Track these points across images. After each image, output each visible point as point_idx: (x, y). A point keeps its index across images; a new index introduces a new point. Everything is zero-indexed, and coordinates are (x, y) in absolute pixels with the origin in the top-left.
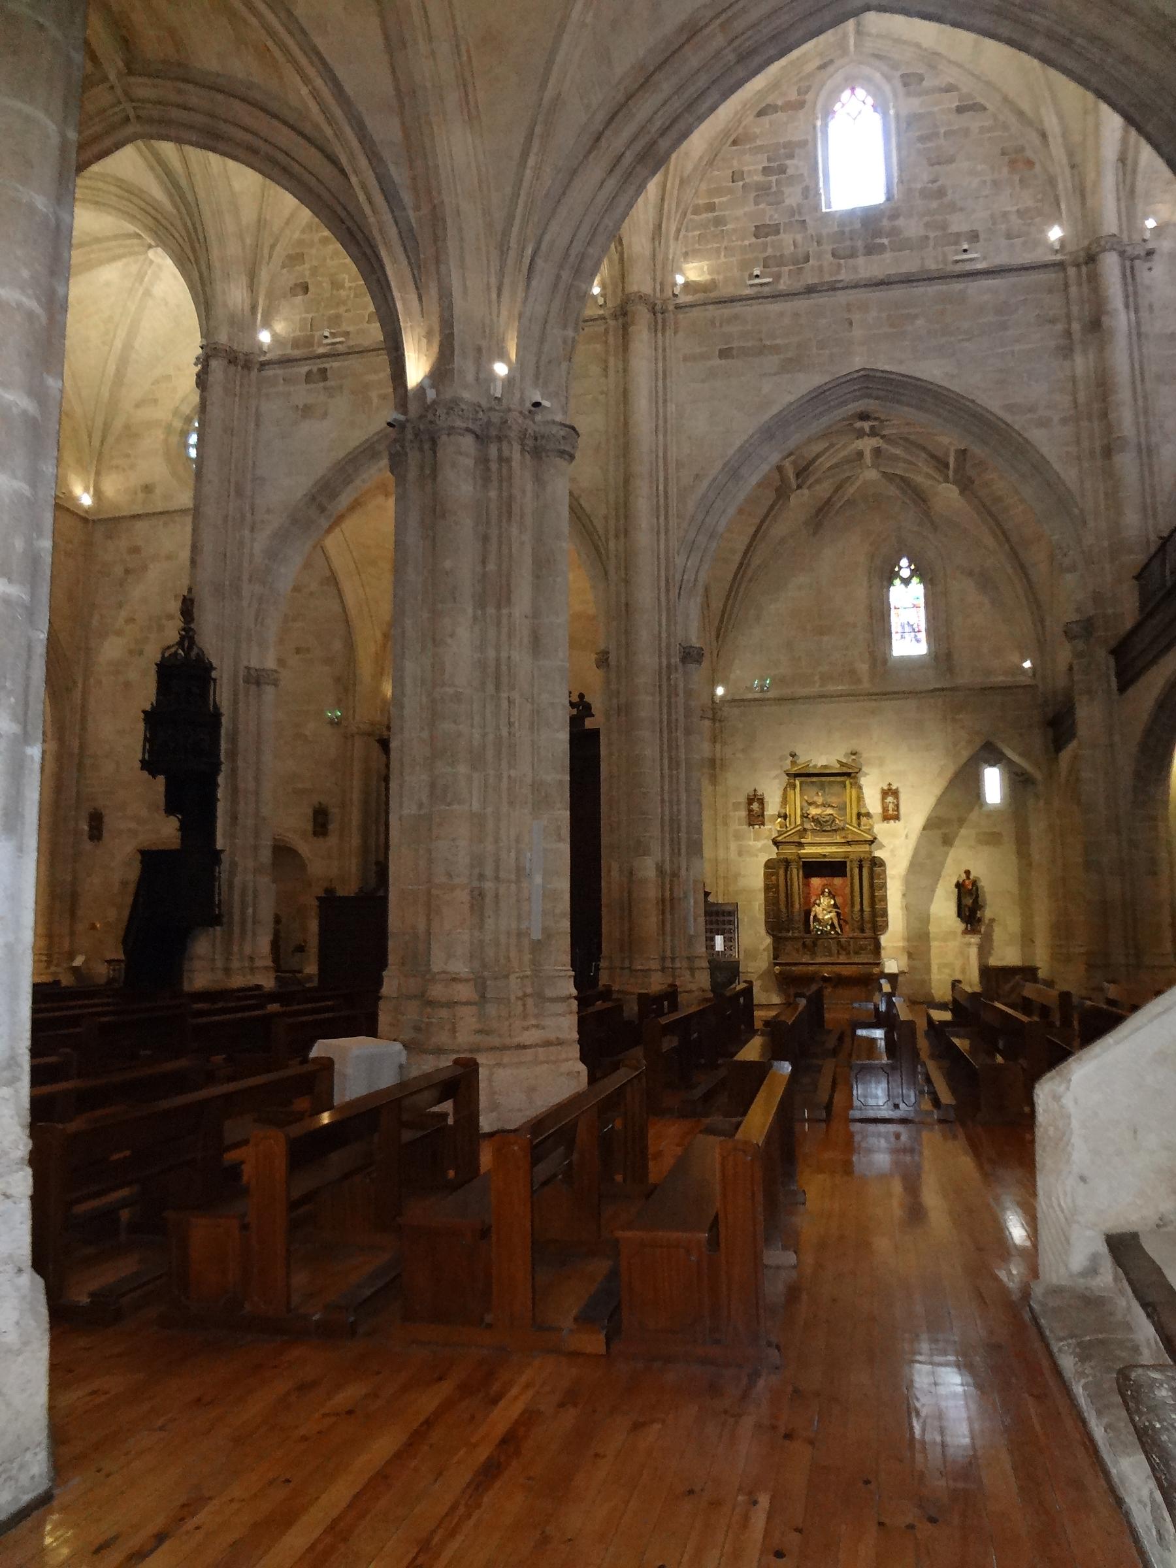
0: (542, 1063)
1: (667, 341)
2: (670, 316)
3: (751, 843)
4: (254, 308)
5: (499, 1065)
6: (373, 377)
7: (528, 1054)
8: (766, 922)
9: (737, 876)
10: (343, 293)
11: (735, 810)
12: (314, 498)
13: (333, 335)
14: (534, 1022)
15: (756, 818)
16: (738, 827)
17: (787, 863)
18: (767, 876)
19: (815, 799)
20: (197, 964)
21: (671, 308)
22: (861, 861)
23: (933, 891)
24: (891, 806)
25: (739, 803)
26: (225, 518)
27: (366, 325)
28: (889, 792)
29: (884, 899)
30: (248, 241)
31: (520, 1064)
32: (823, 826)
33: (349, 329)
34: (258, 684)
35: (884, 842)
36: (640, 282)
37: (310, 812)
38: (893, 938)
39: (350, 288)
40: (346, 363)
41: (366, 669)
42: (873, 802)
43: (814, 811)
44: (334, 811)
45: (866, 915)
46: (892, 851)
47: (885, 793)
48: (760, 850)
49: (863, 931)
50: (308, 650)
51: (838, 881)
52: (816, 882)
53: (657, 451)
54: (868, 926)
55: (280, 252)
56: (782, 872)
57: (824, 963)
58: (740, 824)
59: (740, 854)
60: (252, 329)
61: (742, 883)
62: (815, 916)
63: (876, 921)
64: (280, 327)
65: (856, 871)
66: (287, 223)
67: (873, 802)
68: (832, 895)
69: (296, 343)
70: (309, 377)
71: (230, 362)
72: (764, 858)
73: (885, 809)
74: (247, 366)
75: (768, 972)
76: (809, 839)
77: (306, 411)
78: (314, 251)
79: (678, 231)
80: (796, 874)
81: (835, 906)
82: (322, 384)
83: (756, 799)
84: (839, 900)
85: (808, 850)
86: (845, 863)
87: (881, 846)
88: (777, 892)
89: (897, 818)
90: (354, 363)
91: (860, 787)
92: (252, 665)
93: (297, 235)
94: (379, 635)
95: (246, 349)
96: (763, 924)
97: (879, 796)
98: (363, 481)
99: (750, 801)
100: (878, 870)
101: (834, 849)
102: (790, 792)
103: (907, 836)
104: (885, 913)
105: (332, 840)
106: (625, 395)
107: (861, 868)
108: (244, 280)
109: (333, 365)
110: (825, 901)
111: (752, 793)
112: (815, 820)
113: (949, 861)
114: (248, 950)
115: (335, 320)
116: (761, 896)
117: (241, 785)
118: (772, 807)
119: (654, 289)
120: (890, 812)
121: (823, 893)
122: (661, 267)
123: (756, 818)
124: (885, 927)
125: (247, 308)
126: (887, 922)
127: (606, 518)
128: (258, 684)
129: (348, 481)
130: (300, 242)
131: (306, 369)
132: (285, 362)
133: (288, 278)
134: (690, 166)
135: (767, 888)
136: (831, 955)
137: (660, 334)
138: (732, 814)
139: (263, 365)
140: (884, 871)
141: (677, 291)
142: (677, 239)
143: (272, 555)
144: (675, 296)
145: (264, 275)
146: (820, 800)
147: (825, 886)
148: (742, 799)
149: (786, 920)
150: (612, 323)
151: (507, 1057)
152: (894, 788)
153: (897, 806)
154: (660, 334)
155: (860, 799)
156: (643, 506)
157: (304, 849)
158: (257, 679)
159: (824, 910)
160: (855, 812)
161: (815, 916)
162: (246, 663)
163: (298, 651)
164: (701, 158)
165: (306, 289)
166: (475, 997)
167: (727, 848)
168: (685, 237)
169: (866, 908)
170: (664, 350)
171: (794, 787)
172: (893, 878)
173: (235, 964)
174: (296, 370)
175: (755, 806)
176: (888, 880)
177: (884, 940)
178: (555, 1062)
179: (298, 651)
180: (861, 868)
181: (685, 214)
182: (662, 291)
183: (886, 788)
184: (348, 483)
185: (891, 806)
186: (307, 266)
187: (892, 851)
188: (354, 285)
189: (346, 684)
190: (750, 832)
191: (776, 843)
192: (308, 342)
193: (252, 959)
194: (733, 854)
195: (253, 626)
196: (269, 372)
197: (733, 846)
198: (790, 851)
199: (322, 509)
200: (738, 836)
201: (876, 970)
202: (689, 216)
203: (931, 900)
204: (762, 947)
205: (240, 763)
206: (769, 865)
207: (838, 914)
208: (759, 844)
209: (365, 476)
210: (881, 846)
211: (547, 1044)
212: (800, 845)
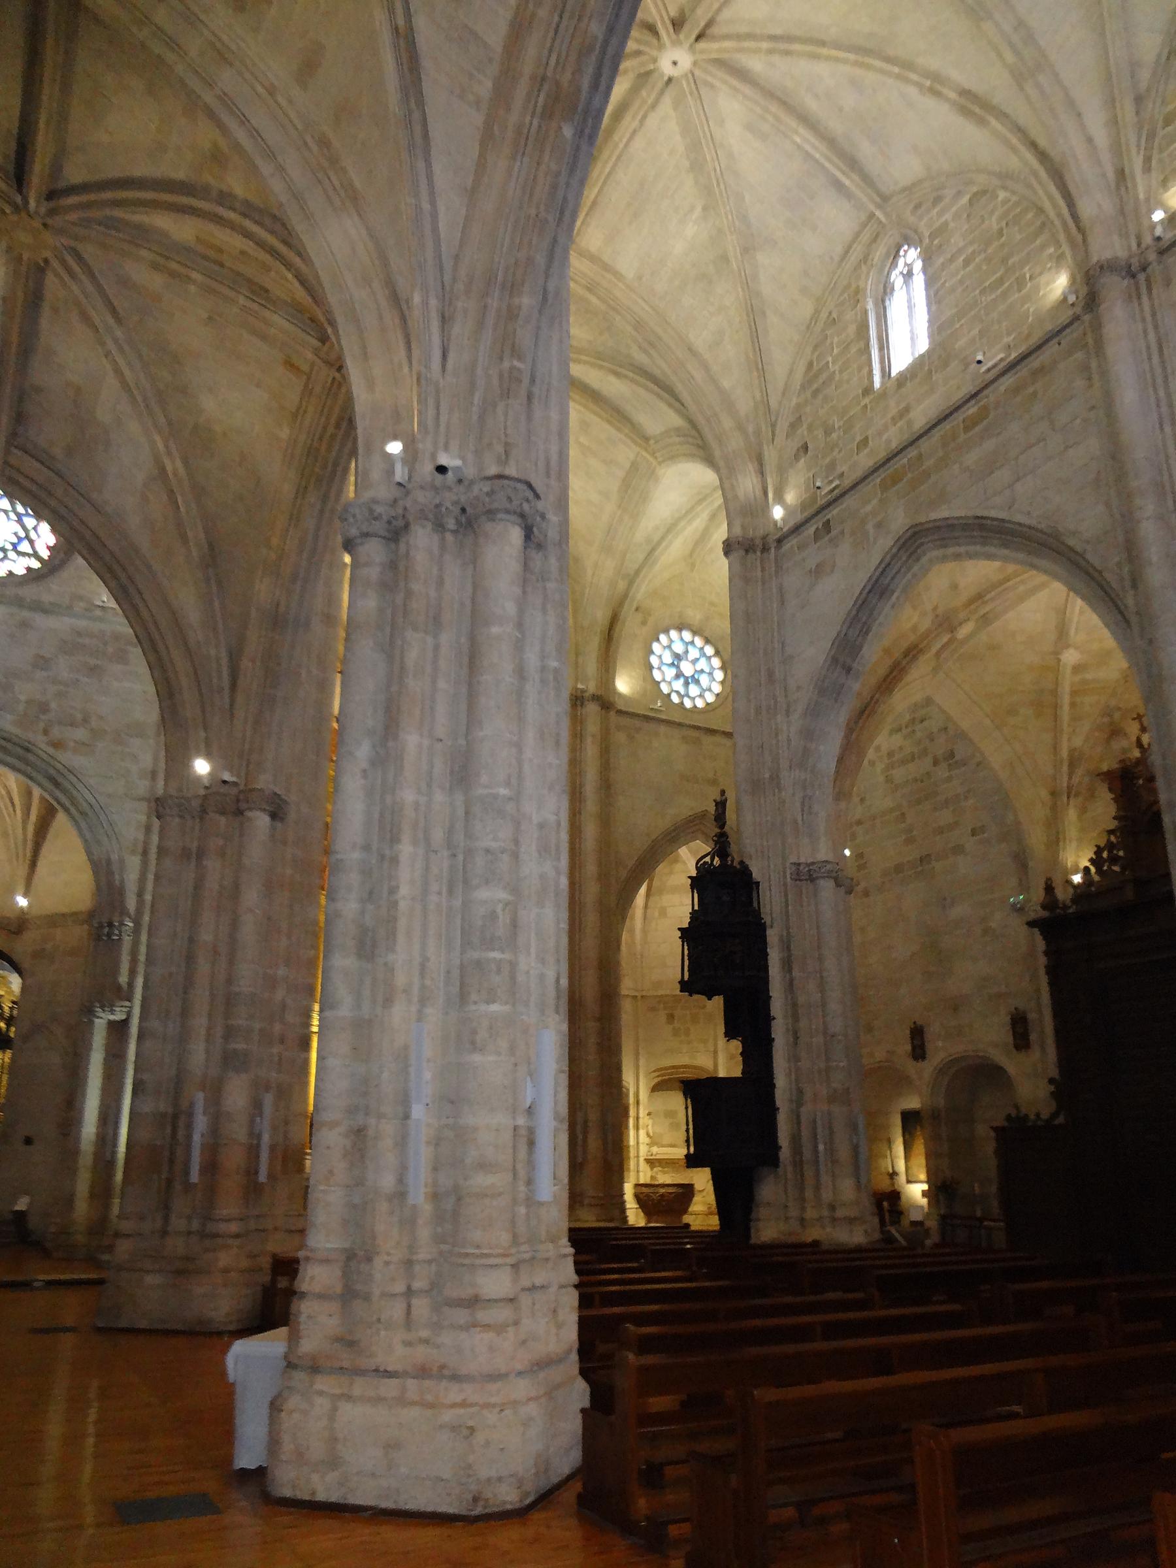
0: (413, 1403)
1: (1156, 302)
2: (1155, 269)
4: (765, 493)
5: (349, 1398)
6: (869, 508)
7: (389, 1388)
10: (834, 435)
12: (835, 660)
13: (831, 482)
14: (424, 1334)
20: (762, 1212)
21: (1152, 256)
26: (758, 710)
27: (856, 457)
30: (750, 429)
31: (379, 1400)
33: (844, 468)
34: (812, 879)
36: (1108, 246)
37: (1008, 1019)
39: (839, 428)
40: (844, 506)
41: (1036, 838)
44: (1032, 1016)
50: (983, 829)
53: (1165, 445)
55: (783, 426)
60: (766, 509)
64: (791, 497)
66: (784, 394)
69: (803, 506)
70: (817, 536)
71: (747, 551)
74: (765, 549)
77: (818, 571)
78: (808, 409)
79: (1148, 160)
82: (826, 539)
90: (850, 501)
92: (802, 860)
93: (794, 401)
94: (1044, 794)
95: (761, 532)
98: (880, 624)
105: (1036, 1054)
106: (1108, 401)
108: (751, 467)
109: (835, 512)
114: (827, 1195)
115: (832, 466)
117: (801, 999)
119: (1129, 247)
122: (1129, 211)
125: (759, 493)
127: (1119, 564)
128: (812, 879)
129: (865, 631)
130: (799, 407)
131: (813, 529)
132: (797, 529)
133: (794, 444)
134: (1145, 75)
137: (1145, 298)
139: (780, 541)
141: (1159, 231)
142: (1147, 169)
143: (808, 734)
144: (1159, 239)
145: (771, 456)
150: (1087, 318)
151: (359, 1387)
154: (1145, 298)
156: (1149, 531)
157: (1012, 1064)
158: (806, 875)
162: (793, 859)
163: (974, 833)
164: (1159, 56)
165: (805, 448)
166: (339, 1289)
168: (1160, 161)
170: (1154, 315)
173: (810, 1213)
174: (806, 534)
178: (431, 1406)
179: (974, 833)
181: (1151, 136)
182: (1139, 245)
184: (867, 633)
186: (805, 426)
188: (841, 423)
189: (1021, 860)
192: (814, 499)
193: (832, 1207)
195: (799, 818)
196: (786, 546)
199: (848, 670)
202: (1161, 133)
205: (796, 973)
209: (881, 619)
211: (422, 1372)
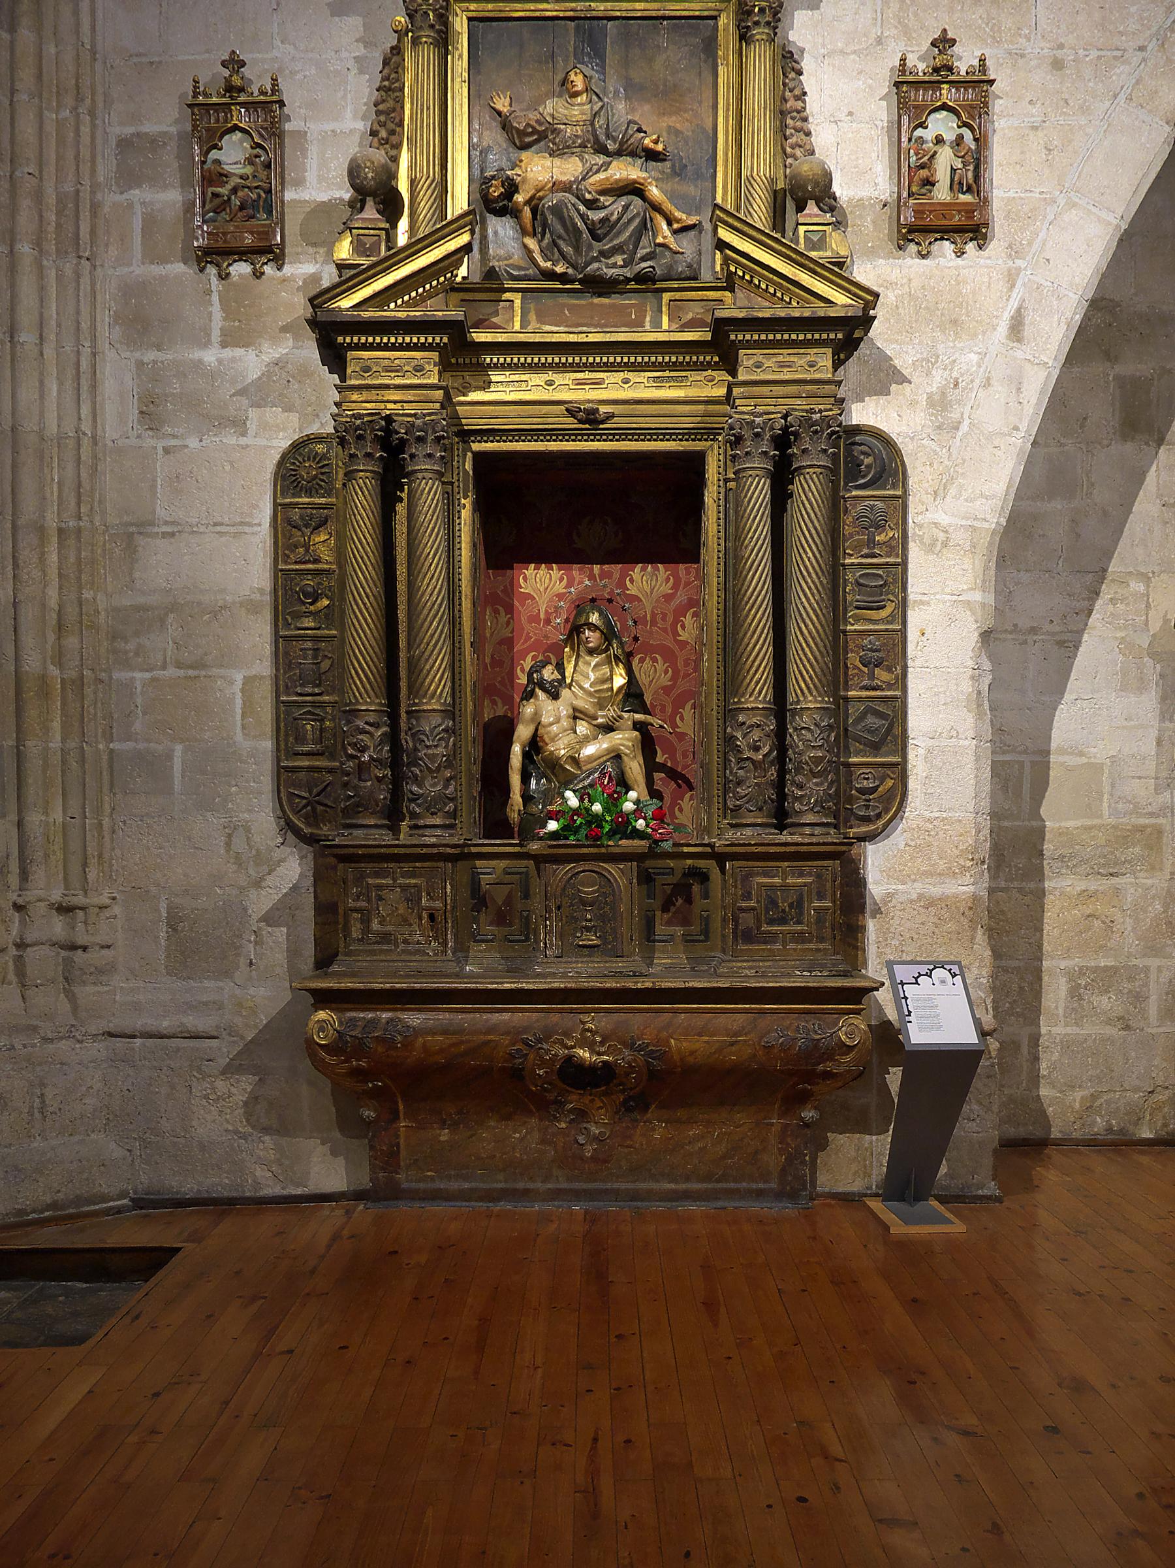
3: (210, 356)
8: (283, 776)
9: (133, 534)
11: (128, 178)
15: (238, 227)
16: (139, 270)
17: (388, 451)
18: (290, 528)
19: (554, 108)
22: (784, 440)
23: (1069, 645)
24: (945, 160)
25: (155, 143)
28: (938, 89)
29: (891, 652)
32: (591, 256)
35: (904, 357)
38: (920, 861)
42: (852, 140)
43: (539, 170)
45: (808, 737)
46: (939, 403)
47: (913, 94)
48: (259, 393)
49: (781, 818)
51: (646, 582)
52: (543, 585)
54: (809, 791)
56: (362, 499)
57: (569, 986)
58: (153, 256)
59: (151, 414)
61: (160, 567)
62: (535, 745)
63: (864, 772)
65: (759, 492)
67: (852, 140)
68: (619, 645)
72: (274, 434)
73: (916, 175)
75: (284, 1031)
76: (516, 322)
80: (444, 525)
81: (633, 696)
83: (236, 106)
84: (653, 675)
85: (508, 390)
86: (696, 461)
87: (886, 378)
88: (335, 616)
89: (971, 229)
91: (788, 62)
96: (266, 783)
97: (881, 112)
99: (209, 117)
100: (862, 498)
101: (641, 386)
102: (417, 69)
103: (1017, 328)
104: (891, 730)
107: (782, 478)
110: (590, 676)
111: (212, 73)
112: (540, 219)
113: (1146, 505)
116: (256, 638)
118: (318, 179)
120: (942, 193)
121: (575, 631)
123: (238, 227)
124: (886, 800)
126: (900, 771)
135: (297, 591)
136: (609, 948)
138: (111, 199)
140: (901, 504)
146: (570, 113)
147: (581, 607)
148: (166, 119)
149: (392, 773)
152: (964, 60)
153: (976, 160)
155: (788, 115)
159: (575, 717)
160: (761, 164)
161: (535, 745)
167: (84, 381)
169: (807, 698)
171: (444, 41)
172: (938, 545)
175: (233, 154)
176: (915, 552)
177: (880, 865)
180: (782, 478)
183: (920, 66)
185: (945, 160)
187: (939, 403)
190: (208, 296)
191: (334, 337)
194: (116, 416)
197: (117, 376)
198: (402, 383)
200: (143, 320)
201: (851, 1029)
203: (1056, 685)
204: (262, 901)
206: (299, 470)
207: (647, 743)
208: (252, 362)
210: (886, 378)
212: (463, 355)
